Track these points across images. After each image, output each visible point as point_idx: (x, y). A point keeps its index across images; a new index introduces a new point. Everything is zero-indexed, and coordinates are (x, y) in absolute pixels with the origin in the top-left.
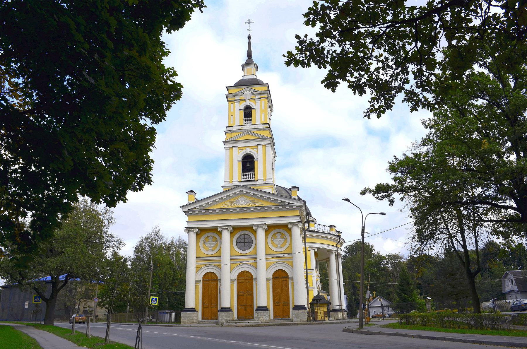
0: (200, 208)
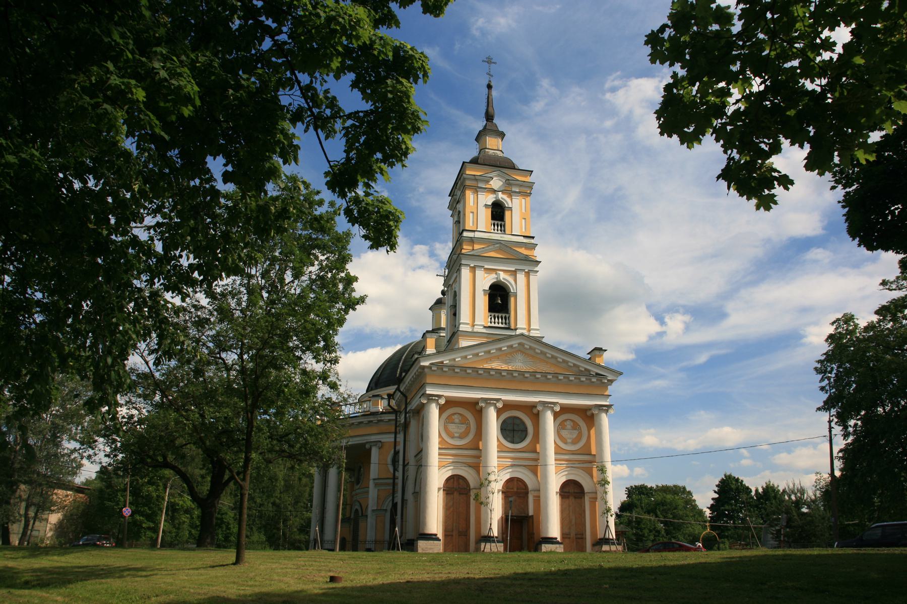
0: (452, 363)
